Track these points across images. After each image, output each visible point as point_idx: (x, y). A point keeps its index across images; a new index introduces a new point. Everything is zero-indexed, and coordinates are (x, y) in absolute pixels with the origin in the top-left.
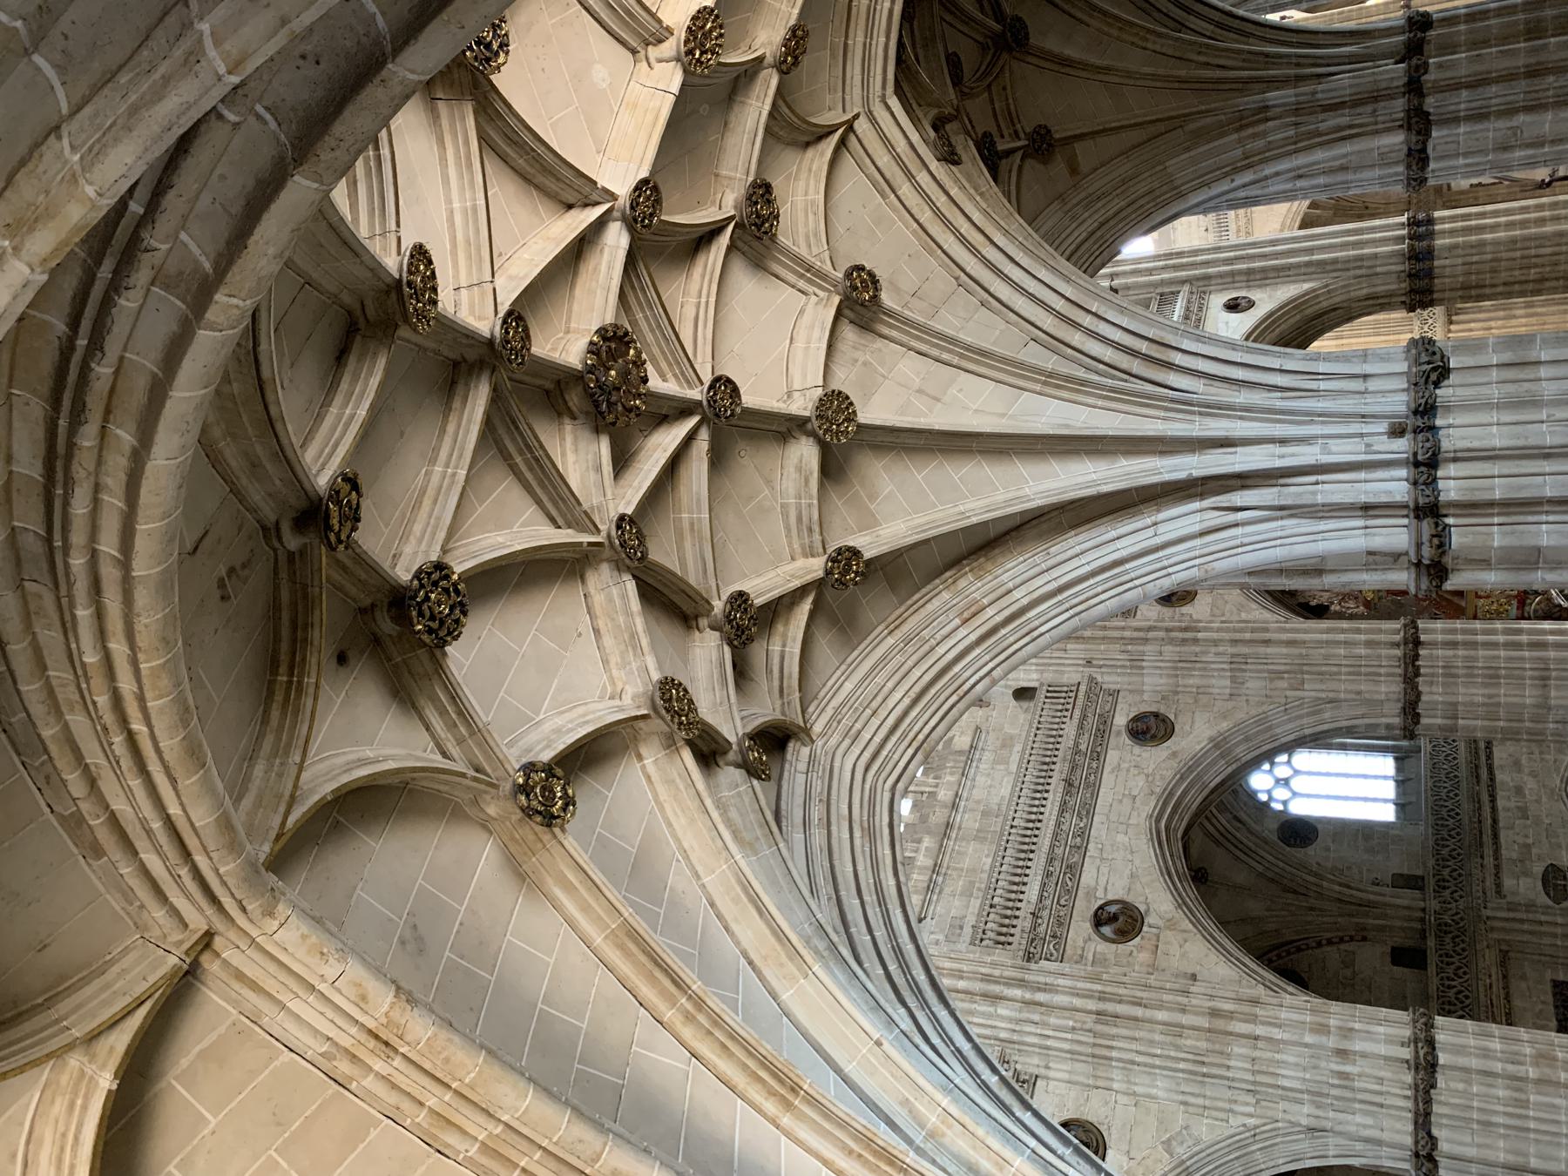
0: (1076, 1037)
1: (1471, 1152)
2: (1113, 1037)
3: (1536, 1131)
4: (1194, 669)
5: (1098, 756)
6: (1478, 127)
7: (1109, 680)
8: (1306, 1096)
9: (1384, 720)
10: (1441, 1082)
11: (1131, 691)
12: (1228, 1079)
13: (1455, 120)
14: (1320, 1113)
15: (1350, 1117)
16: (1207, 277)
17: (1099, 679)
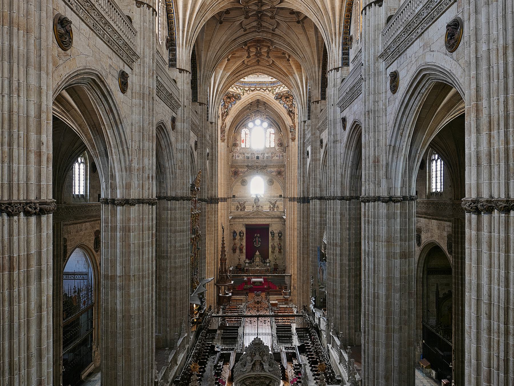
6: (348, 210)
7: (179, 112)
8: (141, 166)
9: (169, 192)
13: (349, 205)
16: (212, 149)
17: (179, 109)
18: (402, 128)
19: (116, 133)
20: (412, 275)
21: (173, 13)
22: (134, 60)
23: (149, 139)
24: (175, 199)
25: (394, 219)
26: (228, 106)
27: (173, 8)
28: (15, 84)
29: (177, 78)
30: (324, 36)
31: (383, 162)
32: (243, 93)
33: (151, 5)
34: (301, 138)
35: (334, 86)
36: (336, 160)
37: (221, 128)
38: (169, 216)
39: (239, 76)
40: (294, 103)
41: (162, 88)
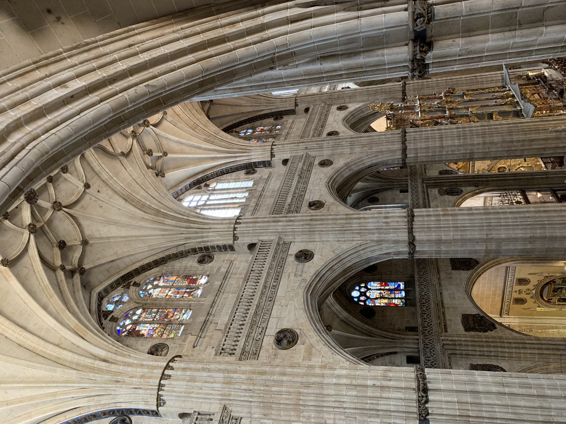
0: (303, 227)
1: (425, 238)
2: (315, 225)
3: (443, 227)
4: (338, 147)
5: (309, 171)
7: (312, 153)
8: (376, 231)
10: (415, 219)
11: (319, 156)
12: (351, 230)
14: (380, 236)
15: (389, 235)
17: (310, 154)
19: (349, 259)
21: (223, 169)
22: (282, 242)
23: (349, 223)
24: (404, 150)
27: (218, 171)
28: (337, 404)
29: (280, 159)
33: (232, 226)
38: (424, 155)
41: (297, 192)
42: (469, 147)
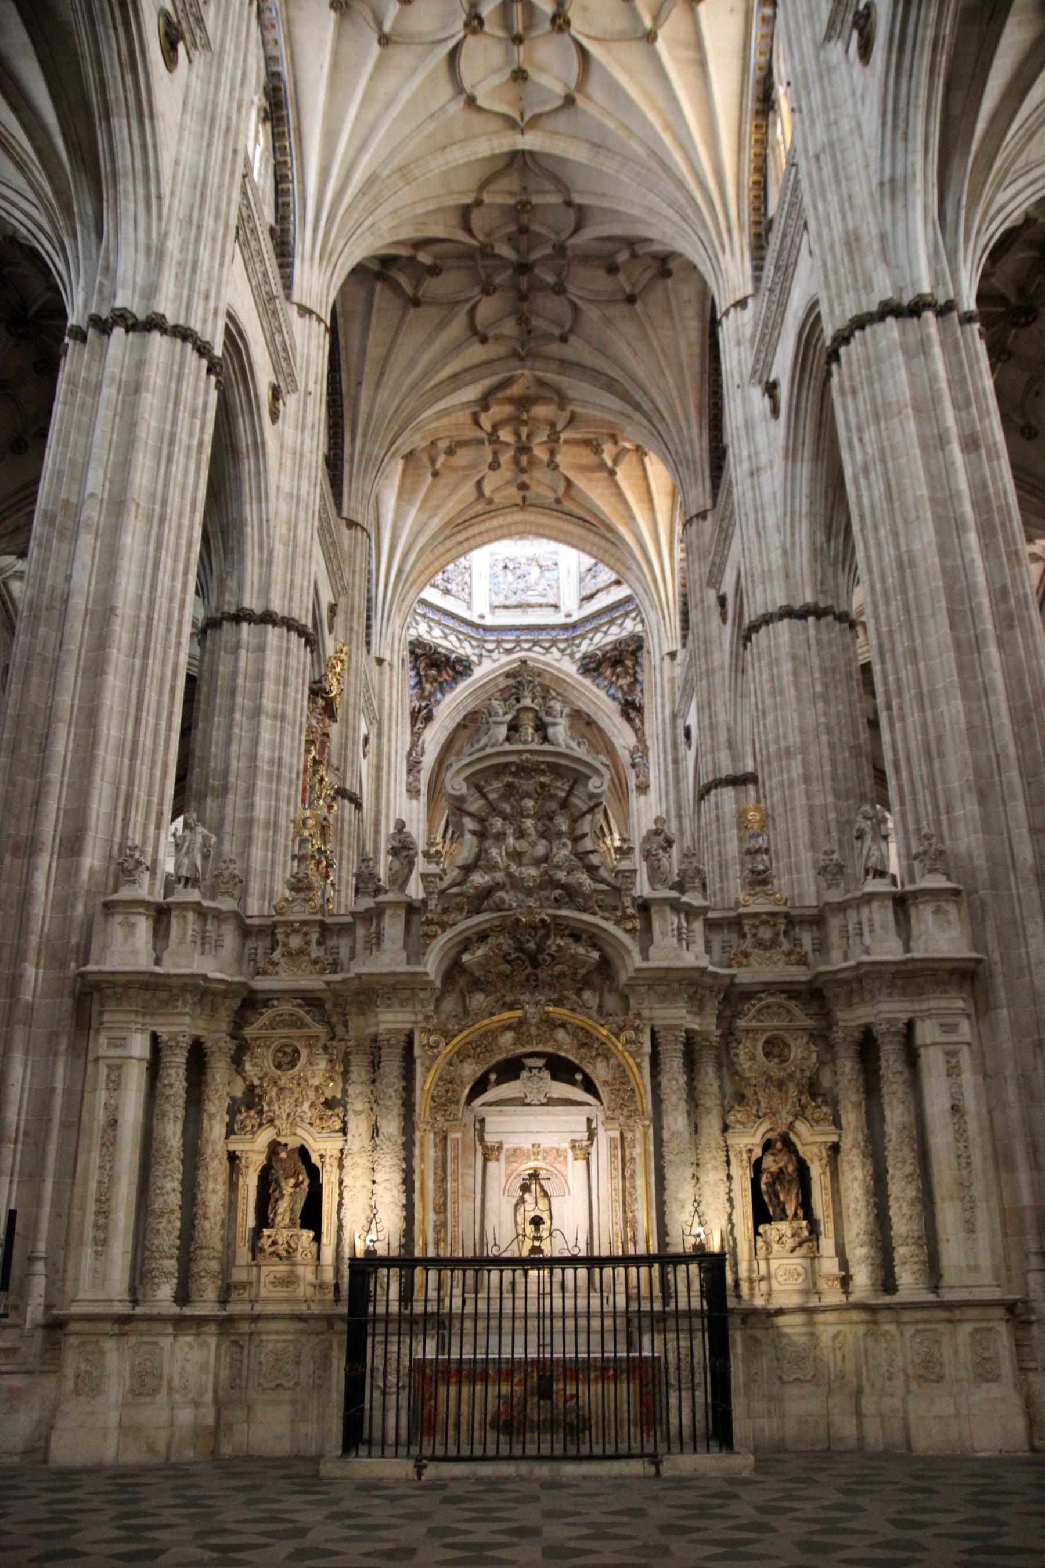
6: (813, 641)
8: (190, 258)
18: (902, 116)
20: (1007, 504)
25: (925, 354)
26: (431, 694)
30: (700, 256)
31: (870, 230)
32: (481, 656)
34: (667, 793)
35: (739, 343)
36: (763, 517)
37: (410, 754)
39: (467, 539)
40: (640, 678)
42: (242, 786)
